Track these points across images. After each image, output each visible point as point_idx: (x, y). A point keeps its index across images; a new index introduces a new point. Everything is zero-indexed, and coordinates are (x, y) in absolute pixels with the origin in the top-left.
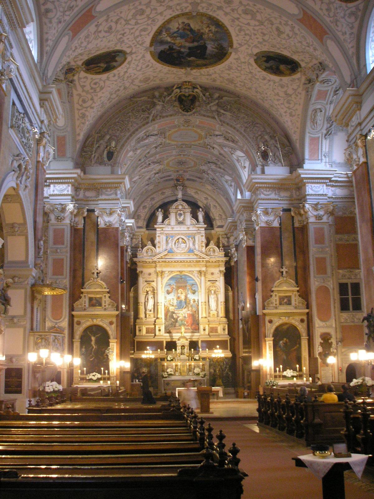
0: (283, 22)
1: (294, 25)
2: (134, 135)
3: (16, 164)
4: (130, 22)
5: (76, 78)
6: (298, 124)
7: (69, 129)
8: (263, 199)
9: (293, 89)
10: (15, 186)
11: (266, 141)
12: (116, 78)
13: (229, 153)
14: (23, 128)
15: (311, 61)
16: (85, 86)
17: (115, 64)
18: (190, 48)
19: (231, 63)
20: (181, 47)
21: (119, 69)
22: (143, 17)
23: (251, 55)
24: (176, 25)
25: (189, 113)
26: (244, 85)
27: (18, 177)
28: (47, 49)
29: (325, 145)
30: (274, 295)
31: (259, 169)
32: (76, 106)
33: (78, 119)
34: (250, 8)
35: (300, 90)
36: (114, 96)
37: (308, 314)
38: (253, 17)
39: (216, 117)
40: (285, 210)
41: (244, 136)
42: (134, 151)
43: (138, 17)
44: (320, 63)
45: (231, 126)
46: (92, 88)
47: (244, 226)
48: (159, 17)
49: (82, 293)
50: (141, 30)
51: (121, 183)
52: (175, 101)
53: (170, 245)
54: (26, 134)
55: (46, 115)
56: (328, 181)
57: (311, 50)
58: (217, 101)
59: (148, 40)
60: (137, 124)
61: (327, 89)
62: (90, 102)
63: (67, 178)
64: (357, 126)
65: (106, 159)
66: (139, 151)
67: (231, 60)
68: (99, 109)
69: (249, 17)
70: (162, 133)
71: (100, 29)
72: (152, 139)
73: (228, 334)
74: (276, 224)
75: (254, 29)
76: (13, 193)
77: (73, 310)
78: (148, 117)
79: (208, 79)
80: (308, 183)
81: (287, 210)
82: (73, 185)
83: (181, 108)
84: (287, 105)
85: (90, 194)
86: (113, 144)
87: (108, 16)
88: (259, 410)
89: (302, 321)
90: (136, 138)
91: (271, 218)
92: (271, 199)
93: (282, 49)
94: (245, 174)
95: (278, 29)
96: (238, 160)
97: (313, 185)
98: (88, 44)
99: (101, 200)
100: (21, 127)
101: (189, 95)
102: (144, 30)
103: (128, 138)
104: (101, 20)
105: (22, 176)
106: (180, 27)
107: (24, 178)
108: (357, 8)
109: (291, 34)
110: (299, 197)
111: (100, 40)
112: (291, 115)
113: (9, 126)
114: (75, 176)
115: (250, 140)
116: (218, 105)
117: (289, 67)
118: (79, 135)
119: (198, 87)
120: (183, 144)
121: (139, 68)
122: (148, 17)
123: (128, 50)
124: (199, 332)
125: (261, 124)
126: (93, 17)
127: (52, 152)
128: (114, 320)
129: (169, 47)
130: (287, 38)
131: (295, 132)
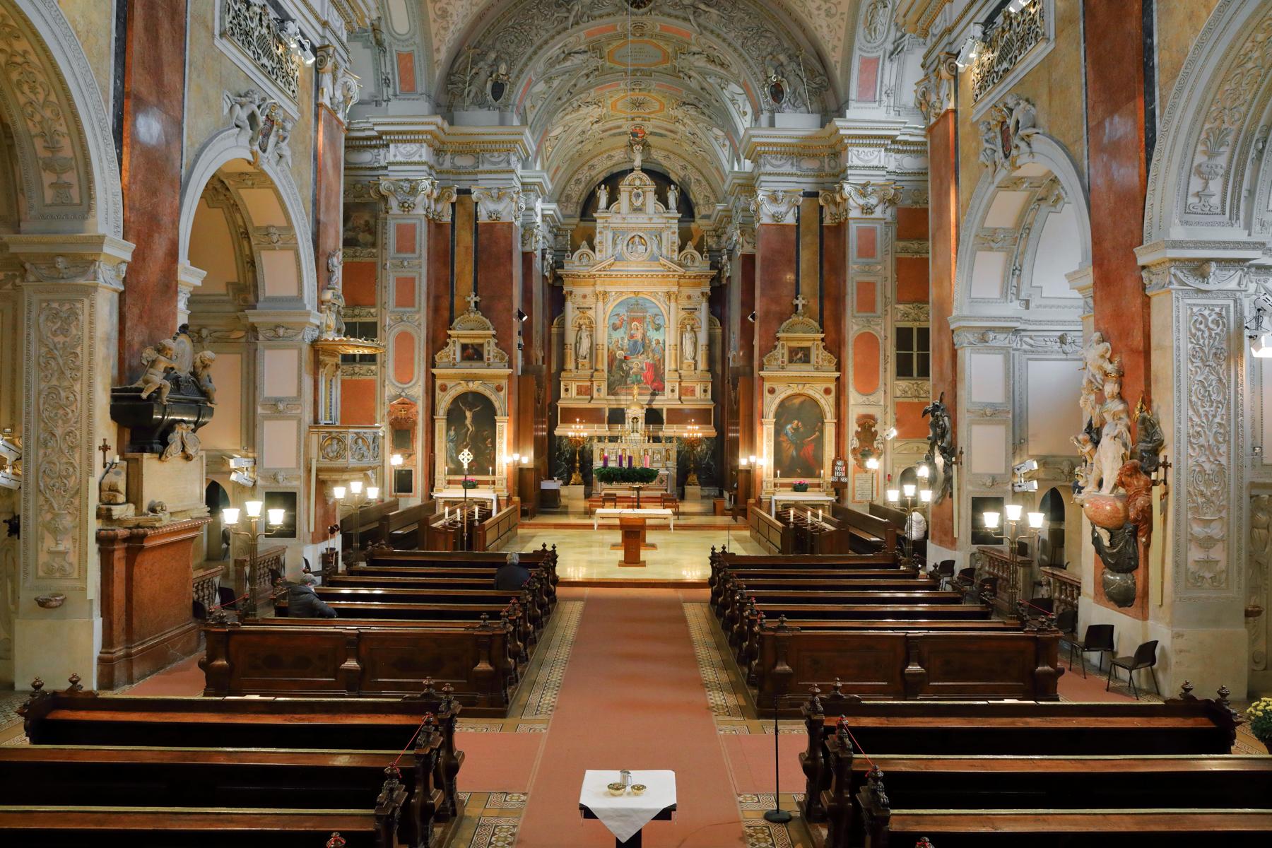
2: (540, 53)
3: (243, 114)
6: (842, 33)
7: (418, 40)
10: (250, 158)
11: (782, 65)
14: (261, 37)
27: (252, 140)
29: (889, 73)
30: (779, 346)
31: (764, 118)
33: (435, 21)
39: (691, 18)
41: (741, 55)
42: (546, 82)
45: (718, 36)
53: (619, 247)
55: (338, 10)
56: (892, 143)
60: (547, 31)
63: (418, 133)
64: (941, 36)
65: (490, 98)
66: (556, 83)
70: (595, 48)
72: (577, 60)
73: (712, 399)
77: (434, 366)
78: (567, 18)
81: (813, 195)
85: (464, 162)
86: (503, 69)
89: (827, 391)
90: (542, 61)
91: (782, 208)
92: (783, 174)
96: (733, 101)
97: (861, 149)
99: (481, 172)
100: (256, 33)
103: (530, 58)
105: (267, 136)
107: (272, 139)
112: (829, 14)
113: (217, 32)
114: (433, 128)
115: (752, 62)
118: (438, 50)
128: (504, 383)
131: (834, 48)
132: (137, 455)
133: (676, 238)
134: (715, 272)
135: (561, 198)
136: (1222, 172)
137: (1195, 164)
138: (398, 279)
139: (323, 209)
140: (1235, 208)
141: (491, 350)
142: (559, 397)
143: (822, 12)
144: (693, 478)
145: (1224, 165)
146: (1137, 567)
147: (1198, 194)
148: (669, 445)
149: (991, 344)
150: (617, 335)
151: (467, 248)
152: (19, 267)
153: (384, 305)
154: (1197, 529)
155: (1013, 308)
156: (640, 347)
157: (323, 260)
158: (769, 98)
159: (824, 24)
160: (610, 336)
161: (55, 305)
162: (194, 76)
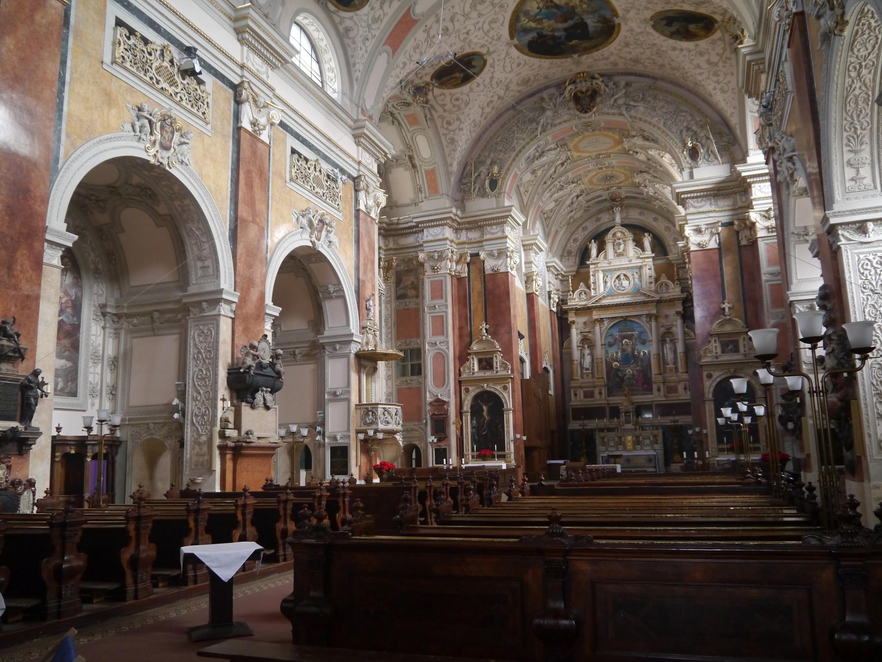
2: (520, 155)
3: (305, 221)
4: (471, 16)
5: (430, 96)
6: (736, 103)
8: (694, 214)
9: (717, 54)
10: (311, 245)
11: (695, 133)
12: (482, 87)
16: (445, 105)
18: (565, 30)
19: (626, 37)
20: (553, 30)
21: (482, 75)
25: (588, 115)
26: (655, 63)
27: (311, 233)
30: (713, 341)
31: (686, 172)
32: (442, 131)
35: (728, 54)
36: (488, 110)
39: (624, 112)
40: (723, 225)
43: (479, 7)
45: (645, 121)
46: (454, 106)
49: (470, 354)
50: (490, 23)
51: (507, 217)
52: (570, 101)
53: (609, 284)
54: (324, 183)
58: (624, 91)
59: (505, 31)
60: (524, 139)
62: (457, 123)
66: (539, 173)
68: (472, 129)
71: (431, 34)
76: (313, 252)
78: (537, 129)
79: (606, 64)
80: (754, 182)
81: (729, 224)
82: (450, 227)
83: (578, 109)
84: (715, 79)
85: (474, 235)
86: (496, 169)
87: (437, 15)
91: (704, 238)
92: (703, 212)
93: (680, 4)
98: (421, 54)
101: (587, 91)
102: (494, 21)
103: (514, 160)
105: (321, 231)
106: (541, 5)
107: (324, 233)
110: (746, 204)
112: (723, 91)
113: (288, 180)
115: (673, 136)
116: (626, 95)
117: (701, 25)
118: (451, 165)
119: (597, 76)
120: (599, 155)
121: (508, 69)
123: (484, 51)
124: (652, 394)
125: (686, 111)
126: (415, 21)
129: (538, 33)
134: (684, 295)
135: (564, 255)
136: (869, 161)
137: (845, 160)
138: (432, 317)
139: (361, 271)
141: (498, 359)
143: (718, 92)
145: (869, 157)
147: (852, 179)
148: (656, 432)
150: (613, 351)
152: (186, 309)
153: (424, 337)
156: (628, 358)
157: (363, 304)
158: (688, 159)
160: (607, 352)
161: (201, 327)
162: (274, 204)
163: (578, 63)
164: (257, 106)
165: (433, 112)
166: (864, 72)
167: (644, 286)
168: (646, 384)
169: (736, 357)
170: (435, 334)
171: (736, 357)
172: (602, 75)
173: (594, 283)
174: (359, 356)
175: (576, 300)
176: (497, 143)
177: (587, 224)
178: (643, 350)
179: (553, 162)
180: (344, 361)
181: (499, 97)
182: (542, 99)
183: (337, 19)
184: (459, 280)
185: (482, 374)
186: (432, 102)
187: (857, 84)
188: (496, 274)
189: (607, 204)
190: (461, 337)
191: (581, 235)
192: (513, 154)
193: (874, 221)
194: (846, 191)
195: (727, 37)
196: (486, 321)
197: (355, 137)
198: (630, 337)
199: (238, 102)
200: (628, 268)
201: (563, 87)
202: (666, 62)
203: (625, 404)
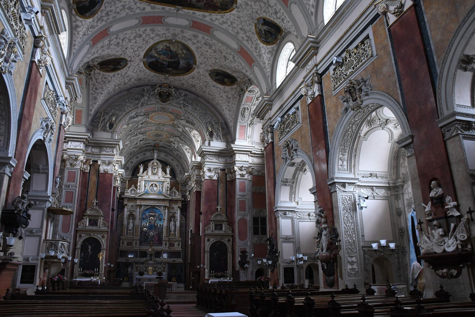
0: (228, 53)
1: (235, 55)
3: (44, 124)
5: (92, 73)
6: (233, 117)
7: (84, 106)
10: (43, 139)
11: (213, 125)
12: (120, 76)
13: (189, 131)
15: (244, 78)
17: (119, 67)
18: (169, 62)
20: (163, 61)
21: (122, 70)
22: (140, 39)
23: (207, 71)
24: (162, 47)
26: (202, 89)
28: (74, 51)
31: (207, 143)
32: (91, 91)
34: (209, 42)
35: (236, 95)
37: (233, 236)
38: (210, 47)
40: (221, 170)
43: (137, 39)
44: (249, 80)
46: (102, 81)
47: (195, 178)
48: (151, 40)
49: (84, 216)
52: (157, 95)
53: (147, 188)
57: (244, 71)
59: (142, 54)
60: (131, 107)
61: (252, 96)
63: (81, 138)
64: (268, 120)
65: (108, 128)
66: (130, 125)
67: (195, 72)
69: (208, 47)
74: (215, 178)
75: (210, 55)
78: (138, 104)
80: (237, 153)
81: (223, 170)
84: (227, 104)
85: (96, 150)
88: (197, 297)
89: (229, 240)
91: (212, 174)
94: (198, 146)
95: (225, 57)
97: (240, 155)
98: (103, 51)
101: (166, 92)
102: (140, 47)
103: (124, 116)
104: (112, 37)
105: (48, 132)
106: (164, 48)
107: (50, 134)
108: (273, 48)
109: (232, 60)
110: (231, 162)
111: (111, 50)
112: (229, 110)
114: (87, 137)
116: (184, 100)
117: (230, 80)
118: (91, 110)
121: (135, 71)
122: (144, 40)
123: (129, 59)
126: (108, 34)
127: (71, 119)
130: (230, 62)
131: (231, 121)
132: (8, 234)
133: (169, 185)
134: (183, 199)
140: (351, 169)
141: (101, 221)
142: (120, 246)
143: (227, 110)
144: (174, 279)
146: (334, 273)
147: (341, 165)
149: (287, 216)
151: (94, 182)
154: (350, 259)
155: (293, 204)
157: (55, 179)
159: (228, 113)
163: (166, 79)
164: (43, 53)
165: (90, 81)
166: (354, 126)
167: (164, 191)
168: (160, 242)
169: (221, 232)
170: (66, 201)
171: (221, 232)
172: (174, 87)
173: (140, 186)
174: (50, 210)
175: (129, 193)
176: (116, 106)
177: (139, 155)
178: (159, 223)
179: (138, 122)
180: (41, 211)
181: (124, 83)
182: (143, 90)
183: (74, 19)
184: (83, 173)
185: (91, 228)
186: (92, 76)
187: (350, 130)
188: (106, 173)
189: (151, 148)
190: (80, 205)
191: (135, 161)
192: (124, 114)
193: (348, 183)
194: (339, 169)
195: (238, 88)
196: (96, 198)
197: (66, 83)
198: (154, 216)
199: (36, 46)
200: (157, 181)
201: (154, 87)
202: (207, 91)
203: (150, 250)
